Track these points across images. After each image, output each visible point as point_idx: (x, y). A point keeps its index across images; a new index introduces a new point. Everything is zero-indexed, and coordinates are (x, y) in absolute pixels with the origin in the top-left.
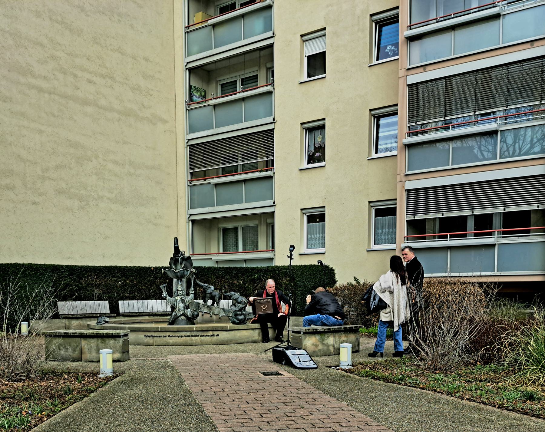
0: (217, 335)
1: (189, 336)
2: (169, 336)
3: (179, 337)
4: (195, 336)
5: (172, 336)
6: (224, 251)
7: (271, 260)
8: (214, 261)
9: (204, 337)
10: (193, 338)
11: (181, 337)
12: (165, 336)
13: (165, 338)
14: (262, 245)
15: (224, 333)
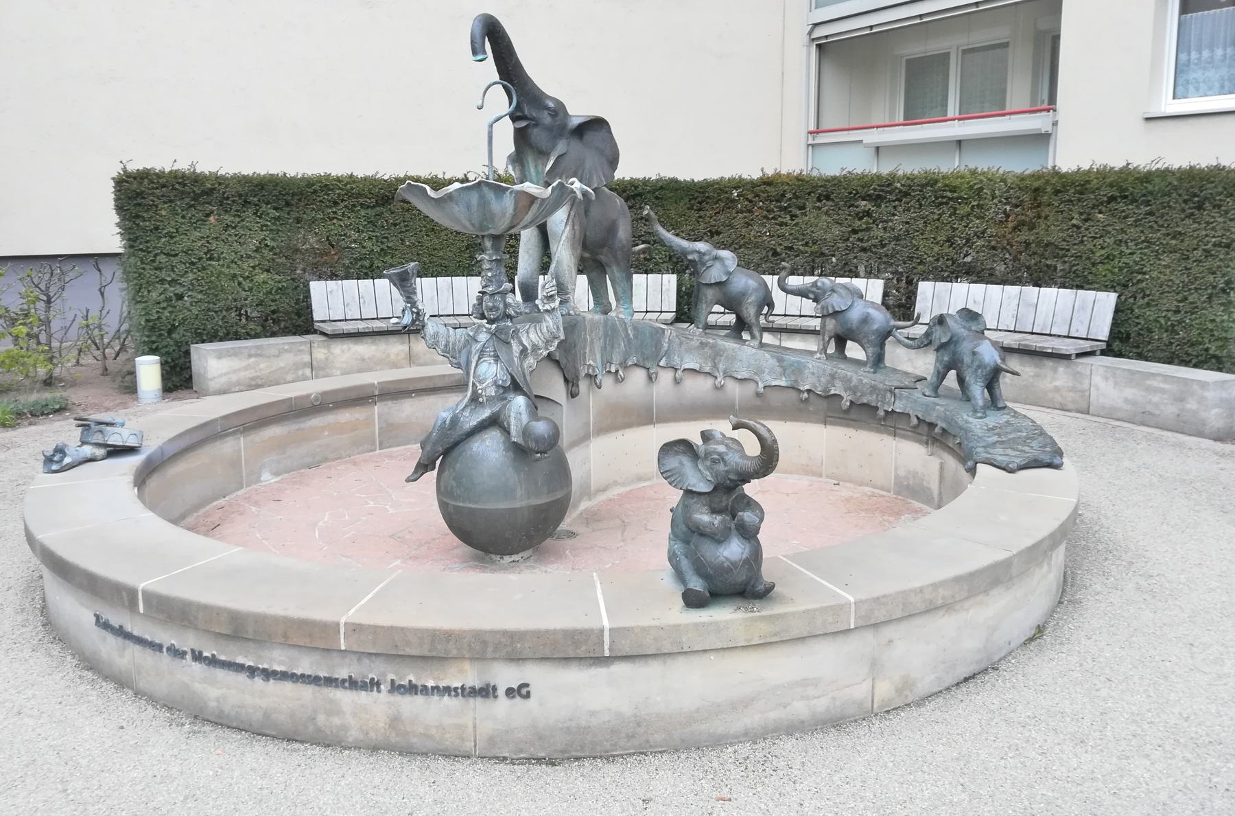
0: (520, 692)
1: (314, 680)
2: (198, 657)
3: (252, 671)
4: (353, 684)
5: (213, 662)
6: (906, 118)
7: (1041, 139)
8: (868, 146)
9: (419, 699)
10: (345, 698)
11: (268, 674)
12: (182, 654)
13: (177, 662)
14: (1018, 94)
15: (574, 676)
